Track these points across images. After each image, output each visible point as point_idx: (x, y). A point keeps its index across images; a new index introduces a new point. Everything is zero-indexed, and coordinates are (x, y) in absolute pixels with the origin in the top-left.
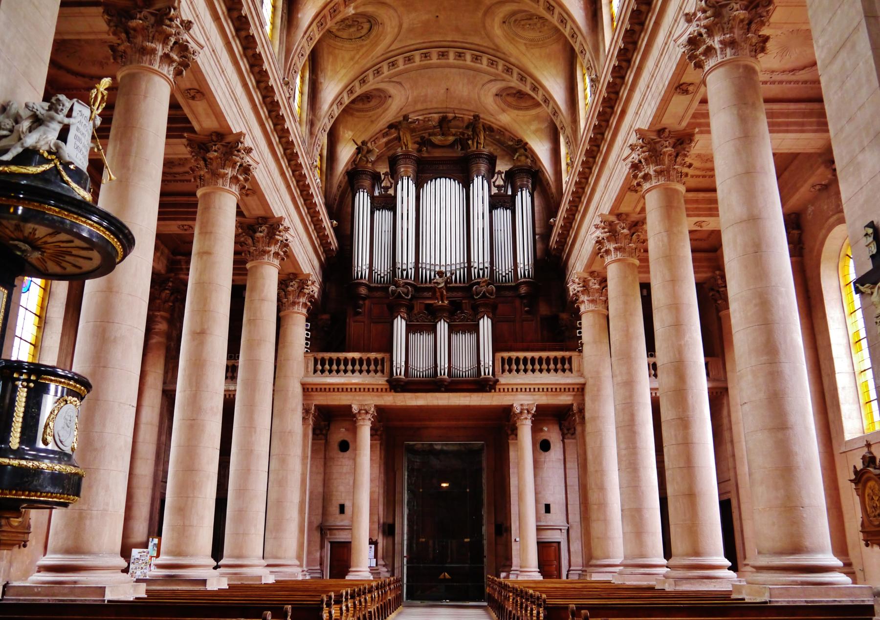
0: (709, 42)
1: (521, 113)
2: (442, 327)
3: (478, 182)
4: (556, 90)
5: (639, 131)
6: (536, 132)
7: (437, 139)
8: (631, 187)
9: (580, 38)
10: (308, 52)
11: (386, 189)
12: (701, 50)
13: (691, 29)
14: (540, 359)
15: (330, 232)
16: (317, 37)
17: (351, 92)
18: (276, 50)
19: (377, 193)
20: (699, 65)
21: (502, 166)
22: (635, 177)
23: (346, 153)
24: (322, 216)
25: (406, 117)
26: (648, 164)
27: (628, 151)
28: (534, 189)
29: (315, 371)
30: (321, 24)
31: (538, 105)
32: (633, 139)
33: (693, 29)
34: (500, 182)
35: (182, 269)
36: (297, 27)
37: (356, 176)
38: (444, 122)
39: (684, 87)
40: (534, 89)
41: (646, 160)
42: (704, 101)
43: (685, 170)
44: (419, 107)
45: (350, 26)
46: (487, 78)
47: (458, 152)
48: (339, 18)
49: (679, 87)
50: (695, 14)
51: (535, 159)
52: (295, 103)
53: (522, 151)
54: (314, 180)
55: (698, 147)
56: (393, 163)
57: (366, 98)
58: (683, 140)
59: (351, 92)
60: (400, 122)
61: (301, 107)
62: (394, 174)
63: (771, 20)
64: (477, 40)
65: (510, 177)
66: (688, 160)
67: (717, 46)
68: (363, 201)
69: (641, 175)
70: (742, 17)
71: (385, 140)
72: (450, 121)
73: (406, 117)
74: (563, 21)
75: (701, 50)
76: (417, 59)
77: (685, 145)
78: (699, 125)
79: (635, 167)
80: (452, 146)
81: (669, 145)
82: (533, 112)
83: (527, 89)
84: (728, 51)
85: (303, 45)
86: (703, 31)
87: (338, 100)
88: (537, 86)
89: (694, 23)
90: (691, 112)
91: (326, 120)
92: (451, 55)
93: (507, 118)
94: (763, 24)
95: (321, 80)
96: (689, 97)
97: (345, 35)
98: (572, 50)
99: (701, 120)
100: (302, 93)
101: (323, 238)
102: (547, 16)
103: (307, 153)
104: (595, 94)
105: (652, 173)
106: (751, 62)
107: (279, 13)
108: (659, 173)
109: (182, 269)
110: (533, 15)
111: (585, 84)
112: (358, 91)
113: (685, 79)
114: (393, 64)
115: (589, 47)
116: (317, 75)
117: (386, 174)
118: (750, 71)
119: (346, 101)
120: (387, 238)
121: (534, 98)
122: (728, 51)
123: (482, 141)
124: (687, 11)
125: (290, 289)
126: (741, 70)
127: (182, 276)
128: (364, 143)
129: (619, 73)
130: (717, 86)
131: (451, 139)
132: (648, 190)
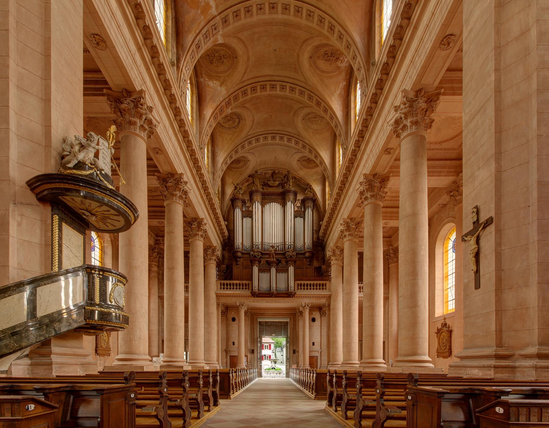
0: (405, 122)
1: (309, 170)
2: (273, 270)
3: (289, 204)
4: (325, 156)
5: (365, 175)
6: (315, 180)
7: (271, 183)
8: (358, 205)
9: (339, 127)
10: (210, 134)
11: (248, 207)
12: (401, 127)
13: (396, 116)
14: (313, 285)
15: (224, 227)
16: (214, 125)
17: (231, 157)
18: (195, 132)
19: (244, 210)
20: (398, 136)
21: (300, 197)
22: (361, 198)
23: (229, 191)
24: (220, 219)
25: (256, 172)
26: (367, 192)
27: (358, 186)
28: (313, 208)
29: (221, 288)
30: (215, 118)
31: (317, 166)
32: (362, 179)
33: (397, 115)
34: (299, 205)
35: (161, 243)
36: (204, 119)
37: (233, 200)
38: (274, 173)
39: (388, 150)
40: (316, 157)
41: (367, 190)
42: (398, 159)
43: (384, 195)
44: (262, 167)
45: (229, 120)
46: (294, 151)
47: (280, 190)
48: (224, 115)
49: (387, 150)
50: (400, 106)
51: (314, 194)
52: (205, 161)
53: (309, 189)
54: (216, 201)
55: (392, 183)
56: (251, 194)
57: (237, 161)
58: (384, 180)
59: (231, 157)
60: (254, 174)
61: (208, 165)
62: (251, 200)
63: (437, 110)
64: (289, 130)
65: (303, 202)
66: (386, 190)
67: (409, 124)
68: (238, 213)
69: (363, 197)
70: (423, 107)
71: (247, 184)
72: (276, 174)
73: (256, 172)
74: (331, 118)
75: (401, 127)
76: (261, 140)
77: (385, 182)
78: (393, 172)
79: (362, 193)
80: (277, 186)
81: (377, 182)
82: (314, 170)
83: (312, 157)
84: (414, 127)
85: (208, 130)
86: (403, 116)
87: (225, 162)
88: (317, 155)
89: (399, 112)
90: (390, 164)
91: (220, 172)
92: (278, 138)
93: (302, 173)
94: (433, 111)
95: (217, 150)
96: (391, 156)
97: (226, 125)
98: (335, 135)
99: (395, 170)
100: (208, 157)
101: (221, 230)
102: (324, 116)
103: (213, 188)
104: (344, 158)
105: (369, 196)
106: (424, 133)
107: (195, 110)
108: (372, 196)
109: (161, 243)
110: (317, 115)
111: (339, 154)
112: (234, 157)
113: (390, 146)
114: (250, 143)
115: (343, 133)
116: (214, 148)
117: (248, 200)
118: (423, 138)
119: (229, 162)
120: (249, 231)
121: (315, 162)
122: (414, 127)
123: (291, 184)
124: (396, 105)
125: (208, 253)
126: (419, 138)
127: (161, 247)
128: (237, 184)
129: (358, 144)
130: (406, 147)
131: (277, 183)
132: (366, 205)
